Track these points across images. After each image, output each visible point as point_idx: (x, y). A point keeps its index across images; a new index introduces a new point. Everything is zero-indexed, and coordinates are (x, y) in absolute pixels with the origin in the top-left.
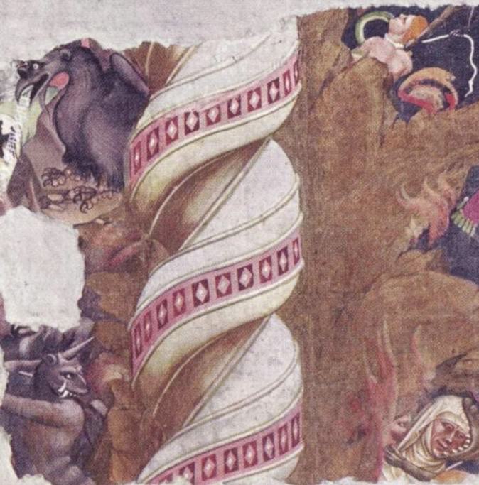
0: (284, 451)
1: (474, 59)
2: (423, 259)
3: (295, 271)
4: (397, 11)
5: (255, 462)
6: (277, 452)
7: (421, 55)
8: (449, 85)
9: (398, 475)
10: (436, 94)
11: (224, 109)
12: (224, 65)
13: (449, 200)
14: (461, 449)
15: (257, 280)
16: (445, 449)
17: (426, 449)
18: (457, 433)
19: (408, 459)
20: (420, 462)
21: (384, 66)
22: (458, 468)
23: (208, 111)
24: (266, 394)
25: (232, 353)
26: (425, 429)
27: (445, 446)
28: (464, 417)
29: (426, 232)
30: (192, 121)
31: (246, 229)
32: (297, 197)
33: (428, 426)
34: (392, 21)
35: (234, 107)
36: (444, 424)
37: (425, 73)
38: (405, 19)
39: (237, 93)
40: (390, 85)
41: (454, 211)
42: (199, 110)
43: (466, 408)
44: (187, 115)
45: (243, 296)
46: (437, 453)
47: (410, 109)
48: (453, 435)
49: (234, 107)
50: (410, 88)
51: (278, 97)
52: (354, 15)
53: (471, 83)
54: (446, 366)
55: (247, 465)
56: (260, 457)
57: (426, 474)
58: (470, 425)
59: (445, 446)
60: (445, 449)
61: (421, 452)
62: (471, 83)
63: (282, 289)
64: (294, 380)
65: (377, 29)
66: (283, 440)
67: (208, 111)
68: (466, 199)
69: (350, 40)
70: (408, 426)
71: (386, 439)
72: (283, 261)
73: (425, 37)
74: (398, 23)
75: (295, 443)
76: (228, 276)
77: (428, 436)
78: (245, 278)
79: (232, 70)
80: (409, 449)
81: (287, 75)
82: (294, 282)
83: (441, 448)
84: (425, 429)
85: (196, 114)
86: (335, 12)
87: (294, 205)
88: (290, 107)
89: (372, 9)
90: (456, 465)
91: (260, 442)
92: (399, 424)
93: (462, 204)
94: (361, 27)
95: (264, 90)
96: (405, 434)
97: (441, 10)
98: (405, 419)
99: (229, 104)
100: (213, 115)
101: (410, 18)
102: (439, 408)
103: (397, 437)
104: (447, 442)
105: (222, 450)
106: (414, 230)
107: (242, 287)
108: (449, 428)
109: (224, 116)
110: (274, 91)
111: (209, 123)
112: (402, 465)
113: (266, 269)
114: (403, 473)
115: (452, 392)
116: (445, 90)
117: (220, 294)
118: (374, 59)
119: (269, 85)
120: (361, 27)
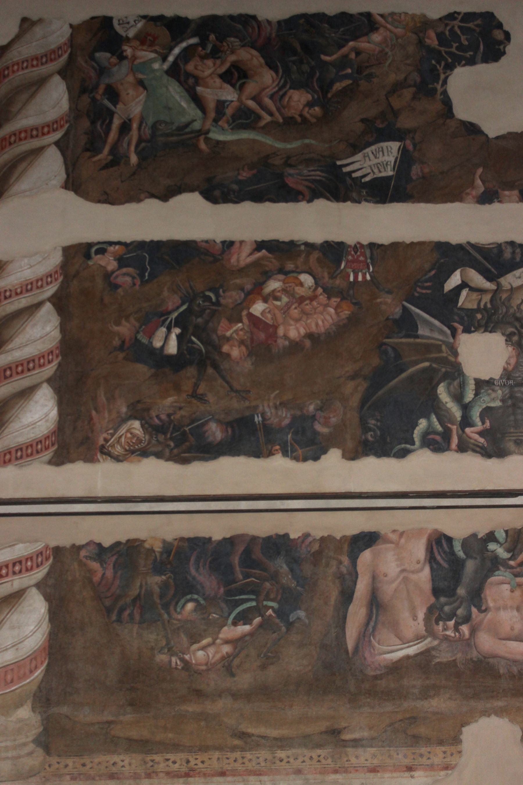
0: (47, 448)
1: (149, 263)
2: (121, 355)
3: (55, 363)
4: (111, 243)
5: (32, 454)
6: (44, 449)
7: (122, 262)
8: (135, 275)
9: (106, 459)
10: (128, 279)
11: (24, 287)
12: (26, 268)
13: (135, 327)
14: (139, 445)
15: (37, 366)
16: (132, 446)
17: (121, 446)
18: (138, 438)
19: (112, 451)
20: (118, 452)
21: (105, 268)
22: (137, 455)
23: (16, 289)
24: (39, 421)
25: (23, 401)
26: (120, 437)
27: (131, 444)
28: (141, 430)
29: (123, 342)
30: (8, 294)
31: (32, 343)
32: (59, 328)
33: (123, 435)
34: (109, 248)
35: (29, 287)
36: (131, 433)
37: (124, 270)
38: (115, 247)
39: (30, 281)
40: (107, 276)
41: (138, 332)
42: (12, 289)
43: (142, 426)
44: (6, 291)
45: (29, 374)
46: (127, 448)
47: (116, 286)
48: (135, 439)
49: (29, 287)
50: (117, 276)
51: (51, 282)
52: (89, 245)
53: (147, 274)
54: (132, 406)
55: (28, 456)
56: (35, 452)
57: (121, 458)
58: (144, 434)
59: (131, 444)
60: (132, 446)
61: (119, 447)
62: (147, 274)
63: (50, 370)
64: (54, 413)
65: (102, 251)
66: (47, 443)
67: (16, 289)
68: (143, 327)
69: (88, 257)
70: (112, 435)
71: (101, 442)
72: (50, 357)
73: (125, 254)
74: (111, 249)
75: (53, 445)
76: (22, 365)
77: (123, 439)
78: (31, 365)
79: (29, 271)
80: (113, 446)
81: (56, 272)
82: (55, 367)
83: (129, 445)
84: (120, 437)
85: (10, 290)
86: (80, 245)
87: (58, 331)
88: (58, 285)
89: (99, 243)
90: (137, 453)
91: (34, 445)
92: (108, 434)
93: (142, 329)
94: (93, 250)
95: (45, 279)
96: (110, 439)
97: (132, 243)
98: (111, 431)
99: (27, 285)
100: (19, 291)
101: (117, 247)
102: (128, 426)
103: (106, 440)
104: (133, 443)
105: (15, 449)
106: (116, 342)
107: (29, 370)
108: (134, 435)
109: (24, 291)
110: (49, 279)
111: (17, 294)
112: (109, 454)
113: (42, 361)
114: (109, 458)
115: (136, 418)
116: (134, 278)
117: (18, 373)
118: (99, 264)
119: (47, 277)
120: (93, 250)
